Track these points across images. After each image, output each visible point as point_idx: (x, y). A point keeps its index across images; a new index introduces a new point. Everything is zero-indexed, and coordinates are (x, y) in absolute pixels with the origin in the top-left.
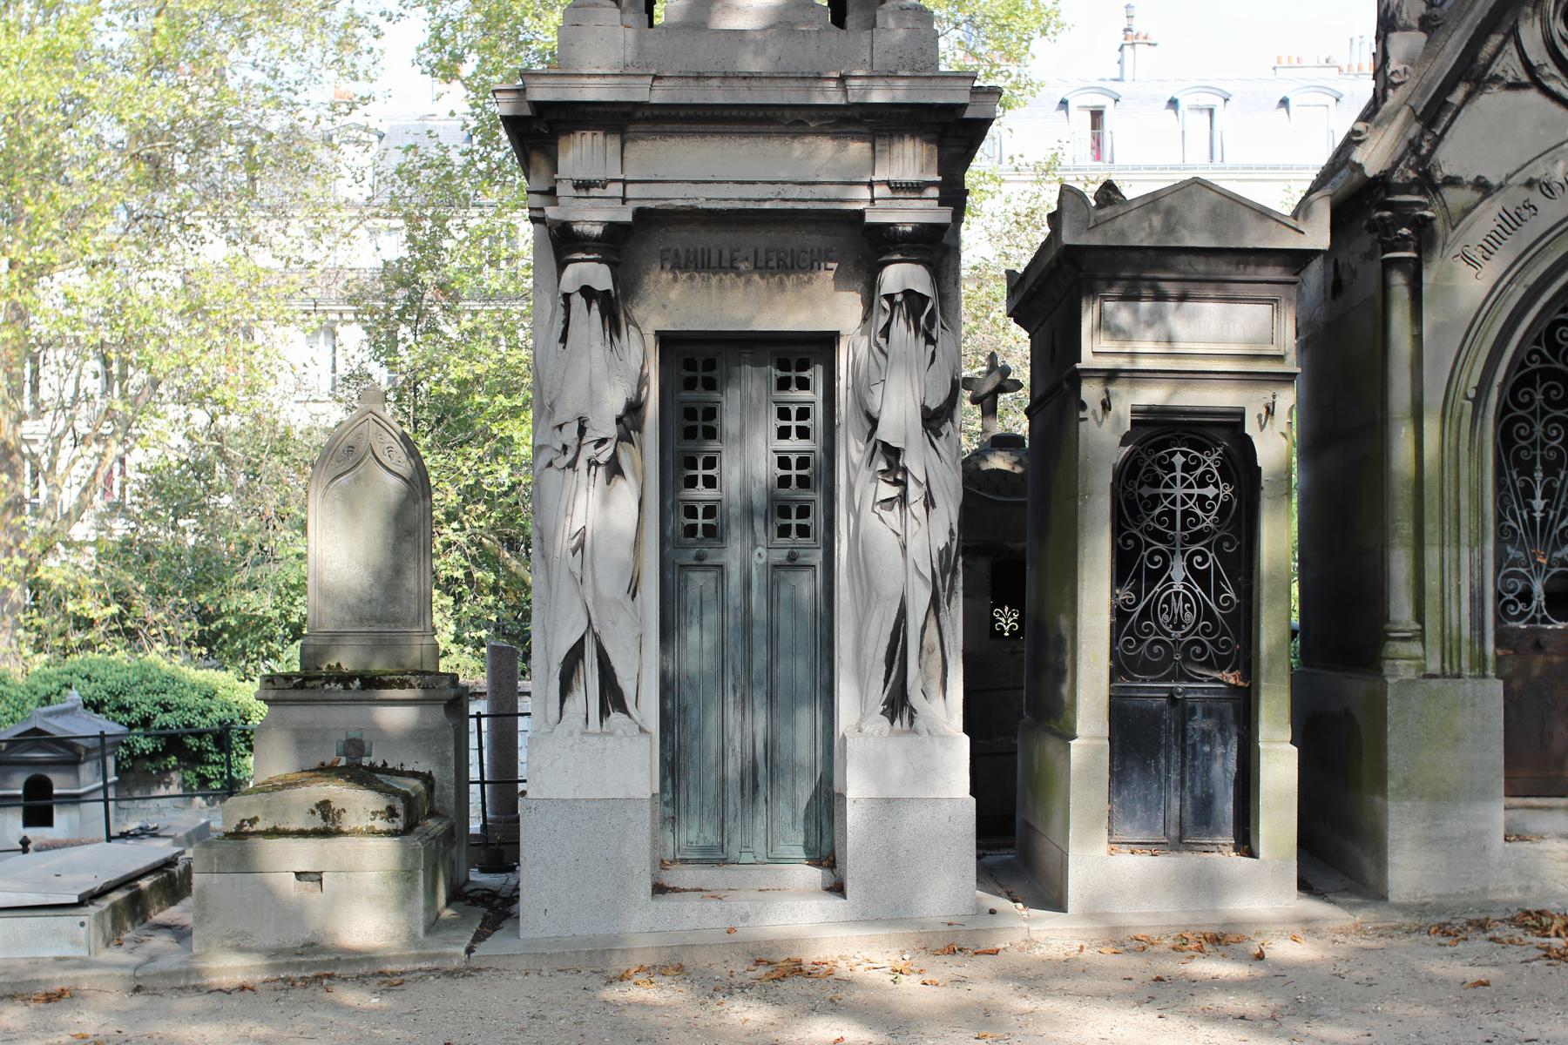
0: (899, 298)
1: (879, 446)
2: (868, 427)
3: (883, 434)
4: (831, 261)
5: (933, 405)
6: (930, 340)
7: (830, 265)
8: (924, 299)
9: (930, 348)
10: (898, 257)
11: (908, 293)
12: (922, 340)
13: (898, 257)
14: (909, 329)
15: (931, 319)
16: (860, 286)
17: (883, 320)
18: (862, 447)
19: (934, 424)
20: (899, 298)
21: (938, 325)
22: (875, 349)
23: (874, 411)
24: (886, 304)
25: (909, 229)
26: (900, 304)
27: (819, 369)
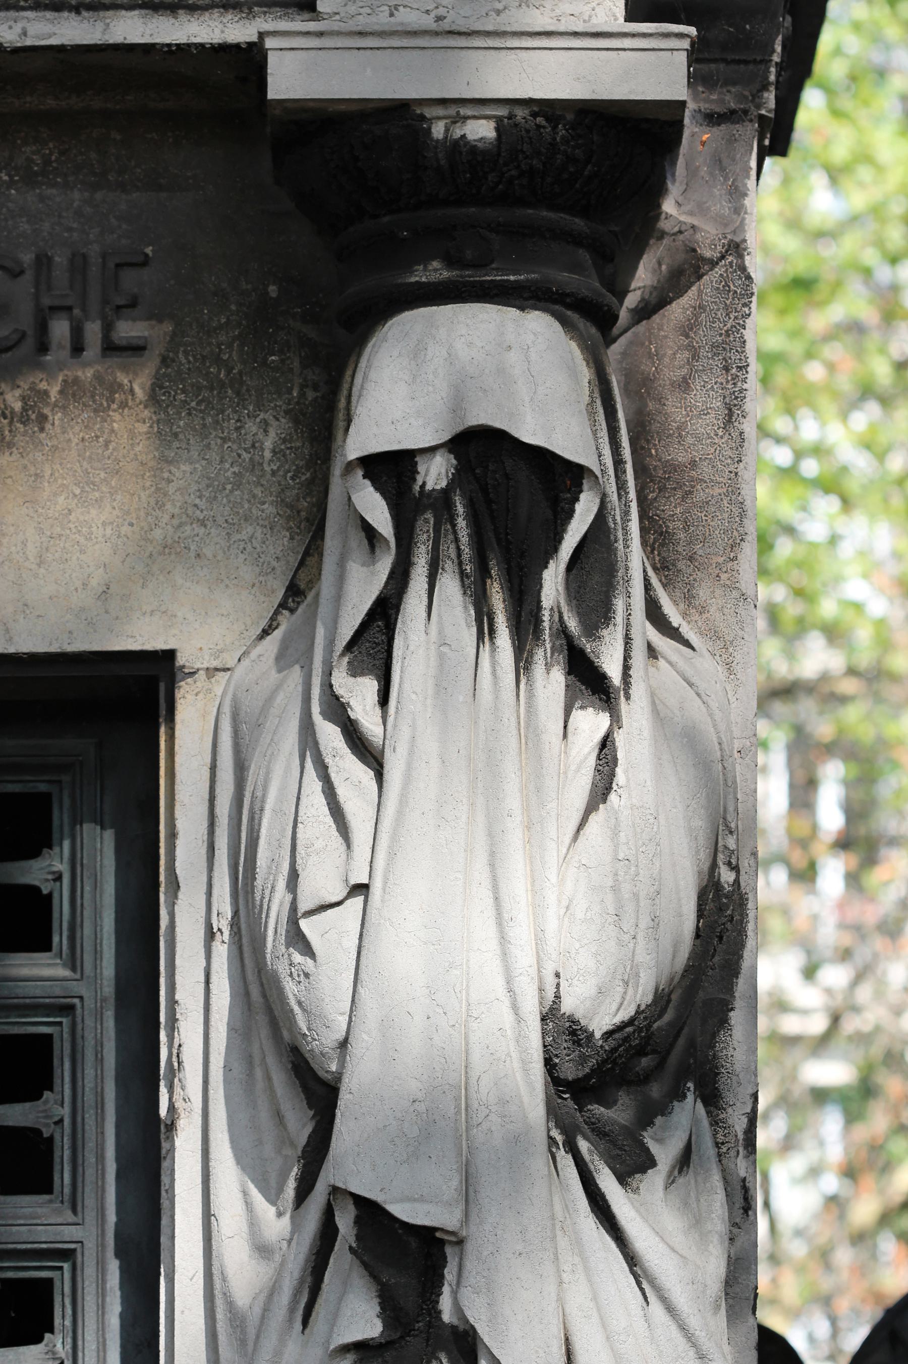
0: (435, 473)
1: (345, 1222)
2: (301, 1129)
3: (355, 1165)
4: (130, 306)
5: (604, 1002)
6: (590, 682)
7: (128, 330)
8: (558, 478)
9: (591, 723)
10: (435, 272)
11: (482, 449)
12: (551, 682)
13: (435, 272)
14: (485, 628)
15: (594, 572)
16: (269, 433)
17: (364, 585)
18: (275, 1224)
19: (618, 1113)
20: (435, 473)
21: (629, 603)
22: (330, 735)
23: (322, 1040)
24: (375, 509)
25: (481, 130)
26: (441, 502)
27: (101, 848)
